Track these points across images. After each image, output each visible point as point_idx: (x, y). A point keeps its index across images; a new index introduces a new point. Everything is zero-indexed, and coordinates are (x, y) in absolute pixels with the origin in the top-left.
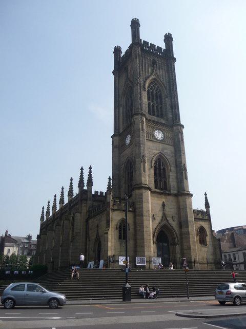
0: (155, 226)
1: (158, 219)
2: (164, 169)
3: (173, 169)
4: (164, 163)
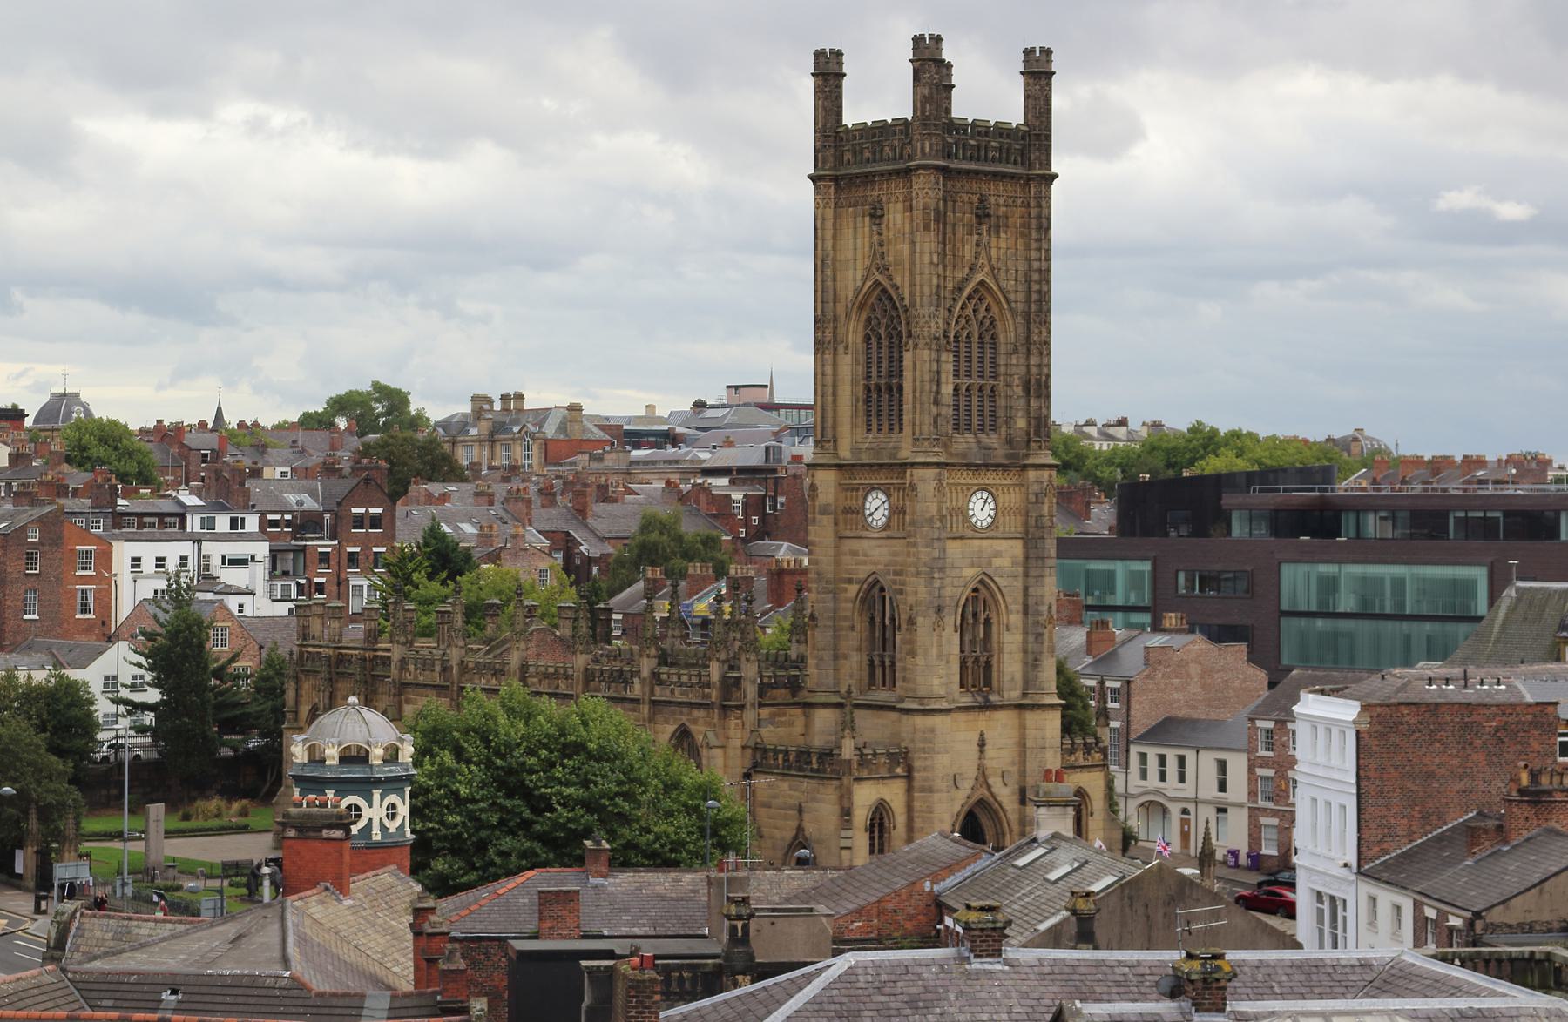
0: (957, 808)
1: (966, 785)
2: (988, 622)
3: (1016, 619)
4: (990, 601)
